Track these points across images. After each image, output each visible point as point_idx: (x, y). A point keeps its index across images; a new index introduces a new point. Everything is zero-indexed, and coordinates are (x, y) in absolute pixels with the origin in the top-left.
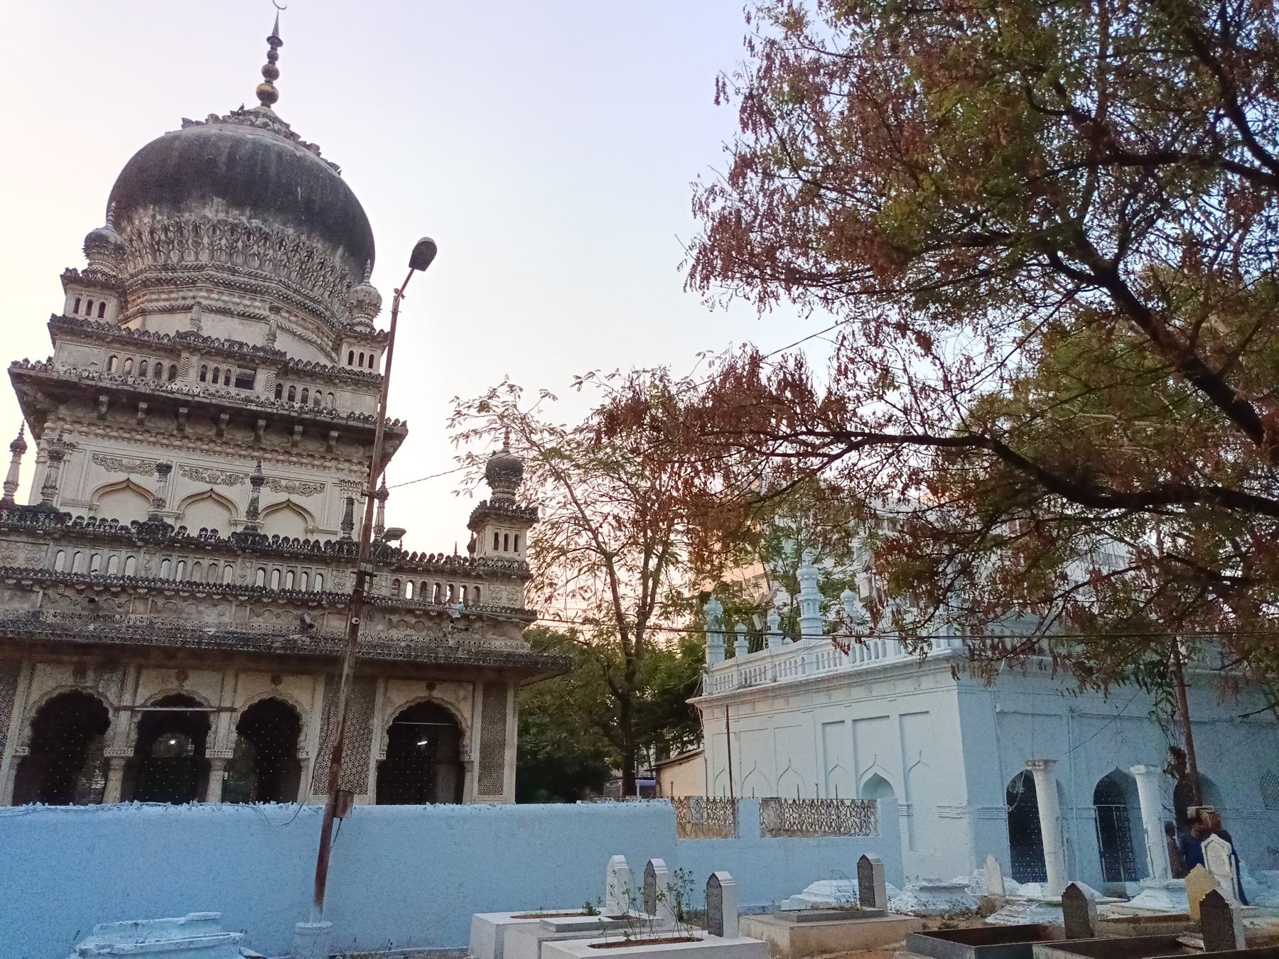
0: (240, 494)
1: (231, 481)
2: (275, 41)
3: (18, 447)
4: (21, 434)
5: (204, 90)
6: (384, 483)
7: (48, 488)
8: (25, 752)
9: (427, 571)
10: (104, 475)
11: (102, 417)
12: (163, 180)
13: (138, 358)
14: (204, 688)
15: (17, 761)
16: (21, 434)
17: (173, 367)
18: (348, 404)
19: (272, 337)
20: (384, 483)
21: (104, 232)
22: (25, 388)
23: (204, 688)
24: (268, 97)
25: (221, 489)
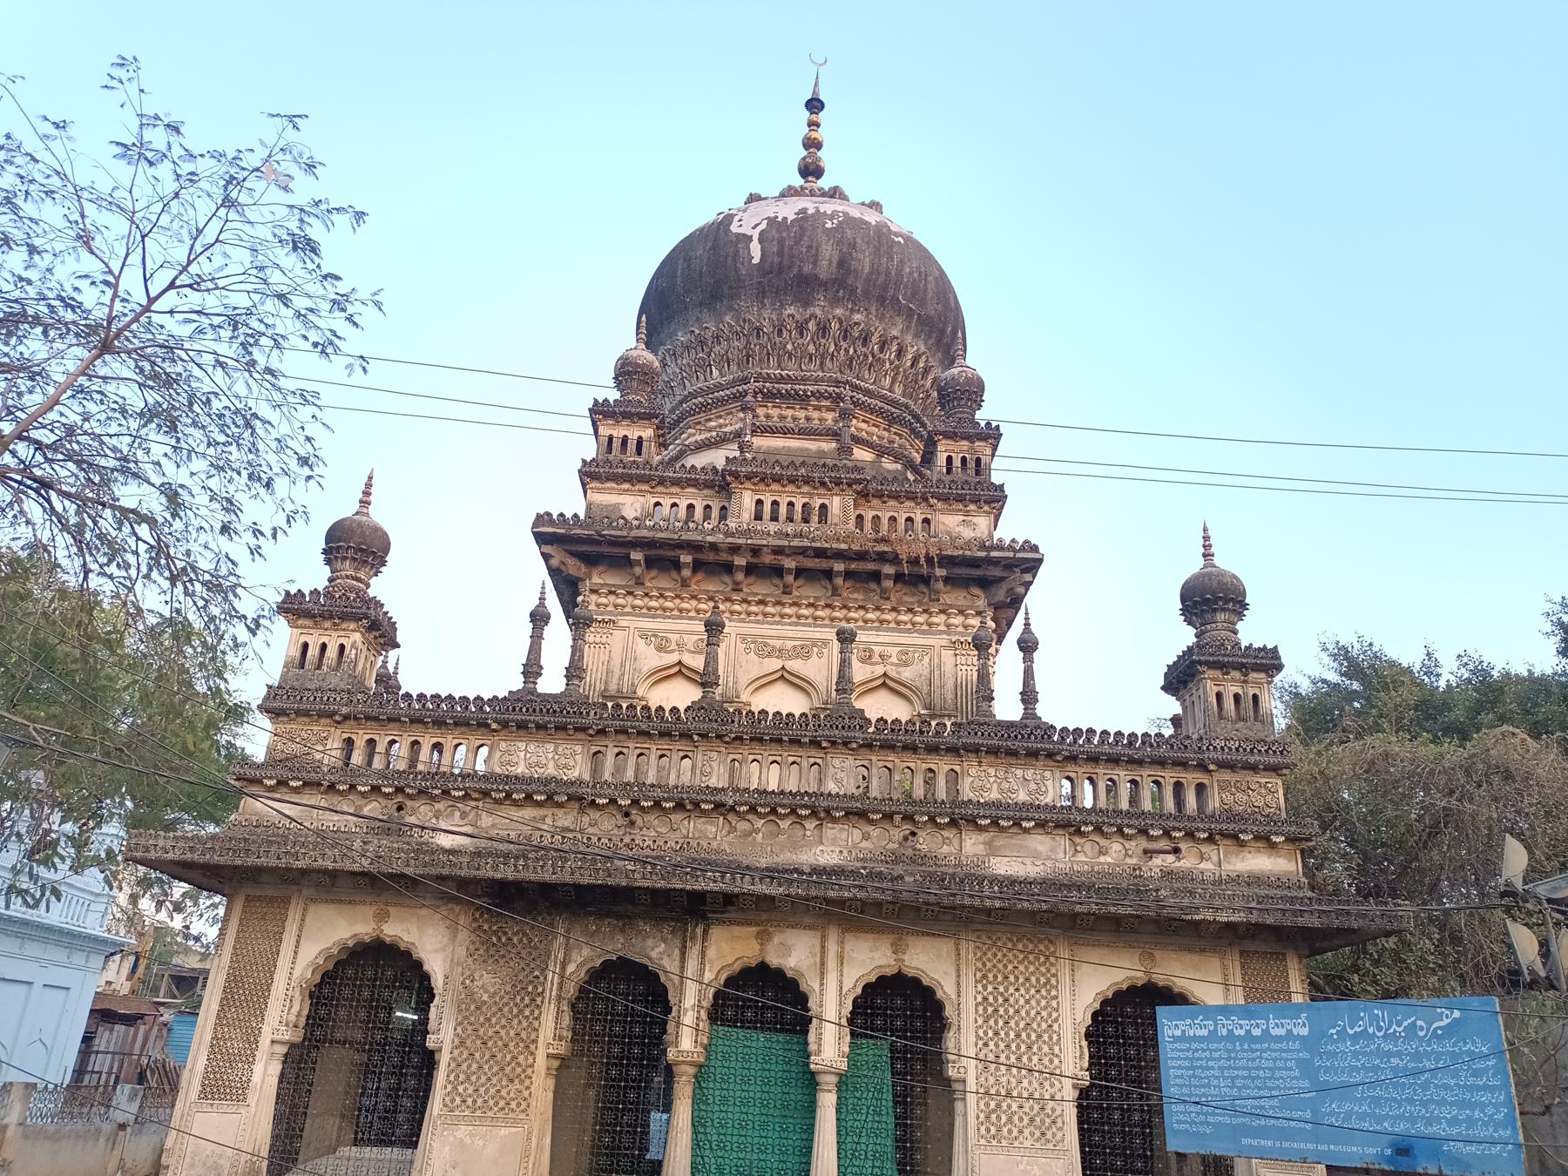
0: (820, 669)
1: (803, 652)
2: (815, 105)
3: (539, 618)
4: (542, 599)
5: (735, 175)
6: (1027, 624)
7: (575, 671)
8: (562, 1048)
9: (1114, 760)
10: (647, 647)
11: (639, 582)
12: (697, 286)
13: (683, 504)
14: (795, 953)
15: (556, 1063)
16: (542, 599)
17: (724, 508)
18: (958, 527)
19: (844, 450)
20: (1027, 624)
21: (634, 353)
22: (548, 549)
23: (795, 953)
24: (810, 170)
25: (794, 665)
